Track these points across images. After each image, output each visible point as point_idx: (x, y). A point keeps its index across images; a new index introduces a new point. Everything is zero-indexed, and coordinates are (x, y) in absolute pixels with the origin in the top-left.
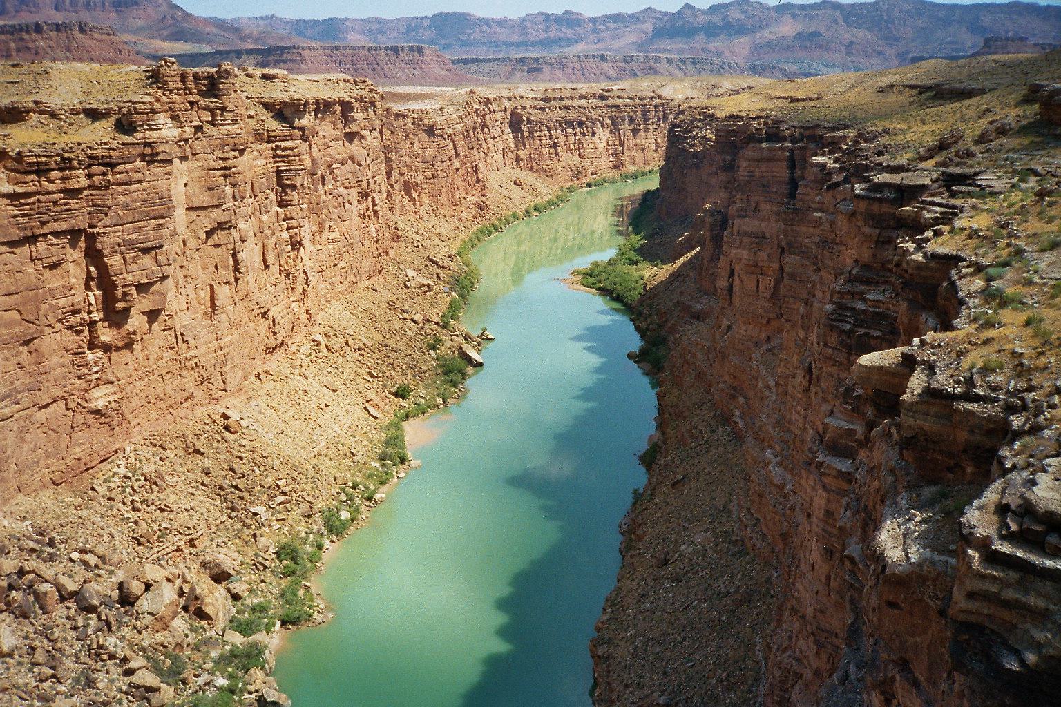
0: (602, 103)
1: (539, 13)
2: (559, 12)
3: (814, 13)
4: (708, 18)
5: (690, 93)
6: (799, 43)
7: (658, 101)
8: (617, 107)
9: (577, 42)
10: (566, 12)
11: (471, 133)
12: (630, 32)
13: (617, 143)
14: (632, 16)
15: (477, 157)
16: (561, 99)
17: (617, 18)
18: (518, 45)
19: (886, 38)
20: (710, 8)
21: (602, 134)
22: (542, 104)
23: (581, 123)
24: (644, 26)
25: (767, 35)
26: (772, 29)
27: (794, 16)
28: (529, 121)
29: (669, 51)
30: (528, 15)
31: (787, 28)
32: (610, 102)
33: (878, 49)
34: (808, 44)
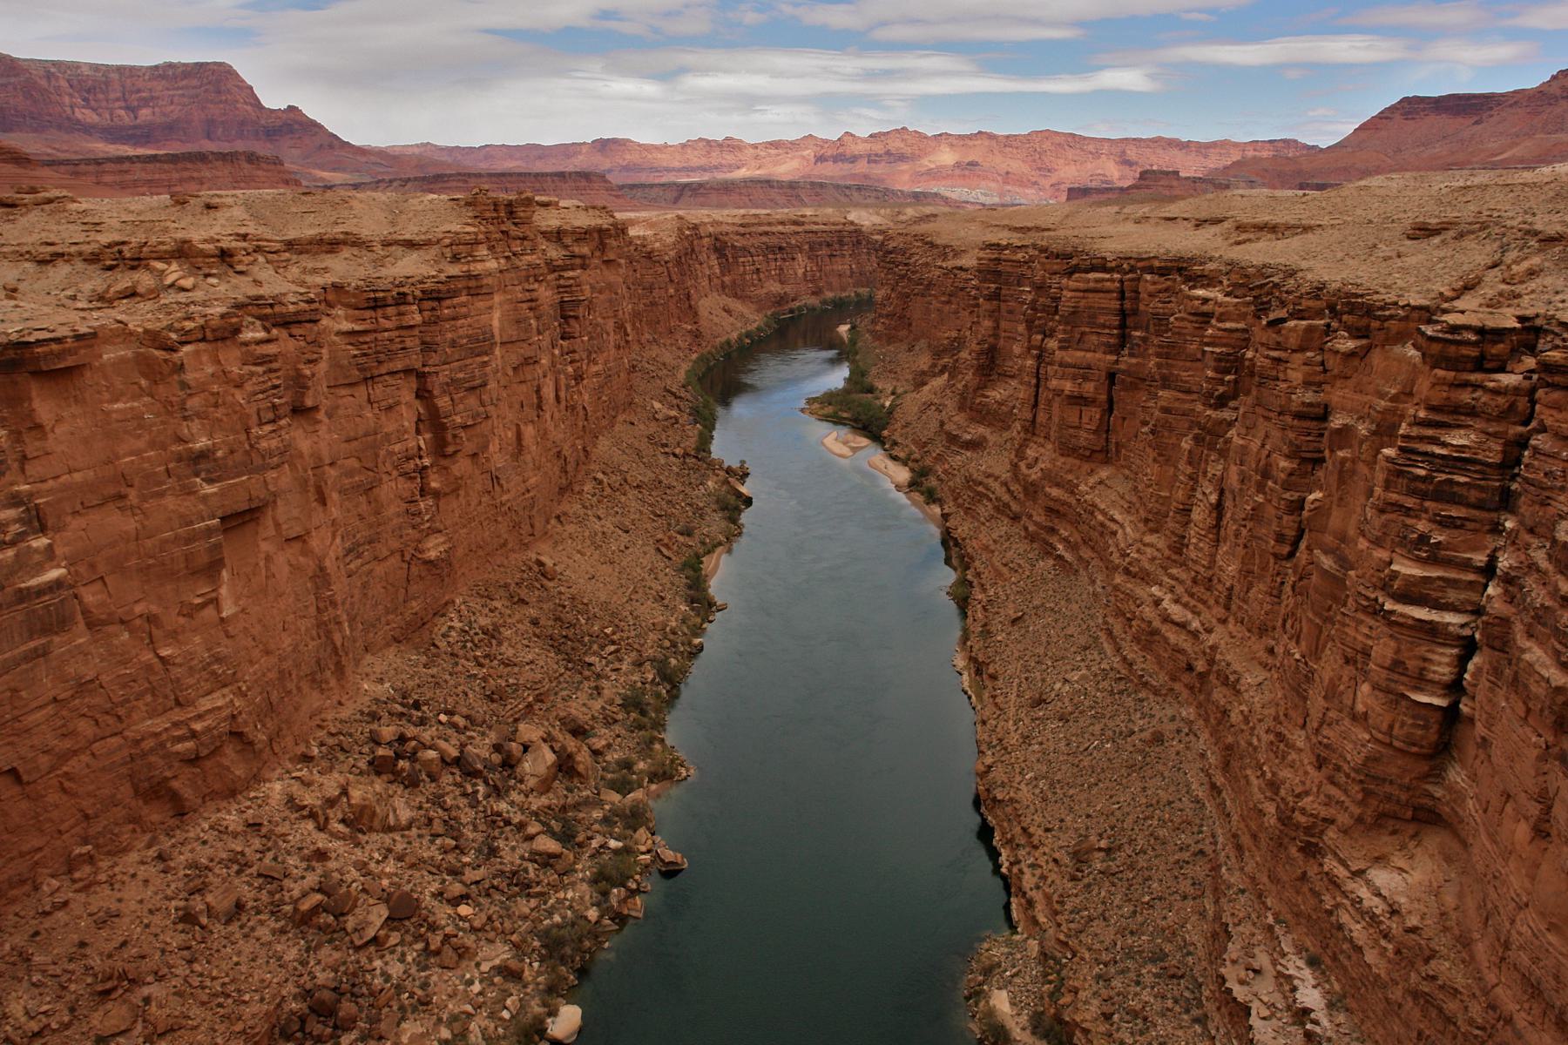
0: (800, 229)
1: (701, 140)
2: (720, 138)
3: (970, 143)
4: (868, 146)
5: (877, 220)
6: (957, 172)
7: (853, 227)
8: (816, 233)
10: (727, 139)
14: (791, 143)
17: (775, 145)
18: (679, 170)
19: (1040, 169)
20: (871, 136)
22: (742, 230)
23: (781, 248)
24: (805, 153)
25: (927, 163)
26: (932, 158)
27: (952, 145)
28: (733, 246)
31: (947, 157)
32: (807, 227)
33: (1034, 180)
34: (967, 173)
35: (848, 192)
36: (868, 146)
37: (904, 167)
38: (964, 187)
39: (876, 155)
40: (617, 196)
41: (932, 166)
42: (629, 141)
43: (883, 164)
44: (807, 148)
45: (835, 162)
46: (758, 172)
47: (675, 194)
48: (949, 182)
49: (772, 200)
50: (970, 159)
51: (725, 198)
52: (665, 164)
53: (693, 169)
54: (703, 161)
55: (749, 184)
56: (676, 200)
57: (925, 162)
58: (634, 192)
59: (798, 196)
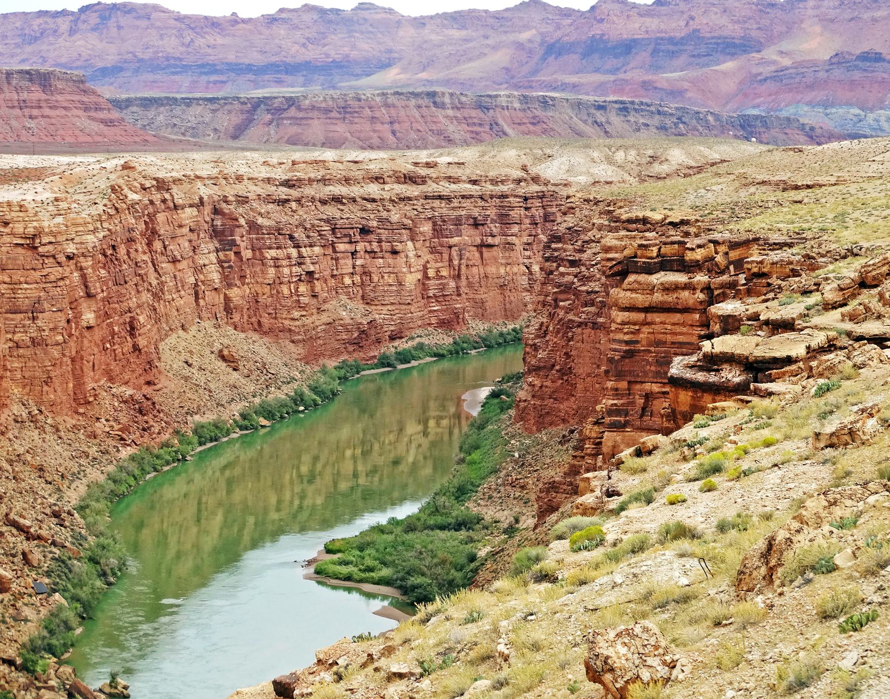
1: (308, 8)
3: (866, 16)
4: (653, 24)
6: (837, 73)
9: (385, 65)
10: (362, 7)
11: (122, 251)
12: (495, 48)
13: (444, 273)
15: (133, 303)
16: (324, 181)
21: (411, 254)
26: (785, 46)
29: (574, 87)
30: (282, 10)
34: (857, 75)
35: (600, 117)
36: (653, 24)
37: (729, 65)
38: (849, 104)
39: (671, 41)
40: (108, 123)
41: (786, 62)
42: (156, 8)
43: (683, 59)
44: (527, 27)
45: (585, 55)
46: (423, 75)
47: (237, 119)
48: (820, 95)
49: (440, 133)
50: (865, 47)
51: (341, 129)
52: (231, 57)
53: (291, 69)
54: (312, 54)
55: (391, 100)
56: (237, 133)
57: (770, 53)
58: (151, 114)
59: (494, 124)
